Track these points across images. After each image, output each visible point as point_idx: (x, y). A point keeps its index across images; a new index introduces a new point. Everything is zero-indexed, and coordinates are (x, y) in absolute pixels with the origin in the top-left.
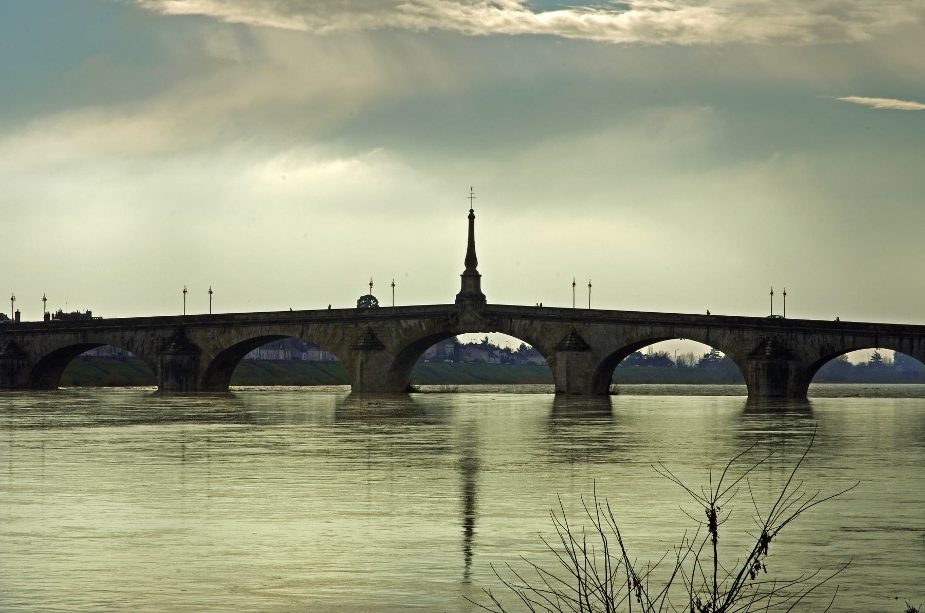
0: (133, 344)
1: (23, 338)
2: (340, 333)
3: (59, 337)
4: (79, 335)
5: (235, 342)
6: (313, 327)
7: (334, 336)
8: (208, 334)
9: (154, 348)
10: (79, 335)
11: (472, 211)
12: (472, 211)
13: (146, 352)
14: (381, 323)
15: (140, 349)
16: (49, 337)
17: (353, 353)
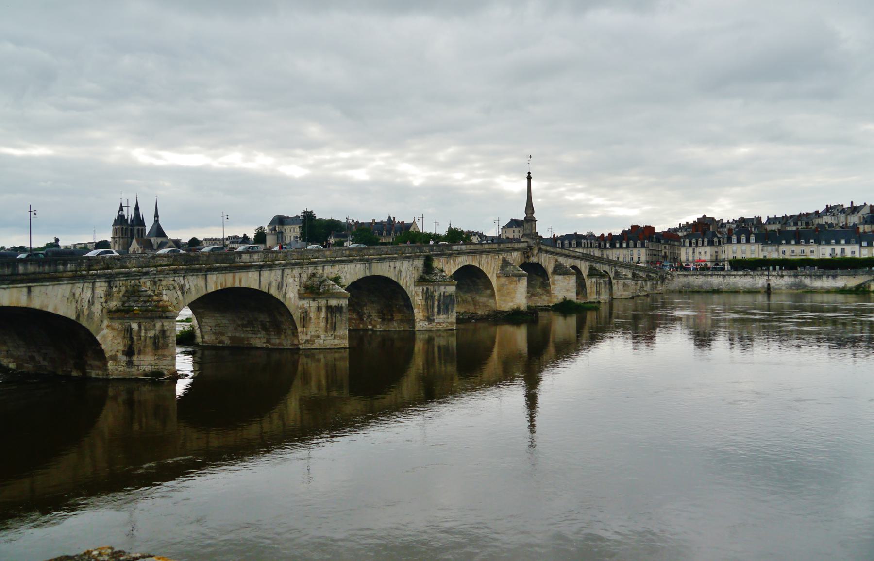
0: (401, 275)
1: (323, 270)
2: (493, 262)
3: (352, 266)
4: (366, 265)
5: (453, 271)
6: (484, 256)
7: (491, 266)
8: (441, 263)
9: (413, 279)
10: (366, 265)
11: (529, 173)
12: (529, 173)
13: (408, 285)
14: (506, 254)
15: (405, 281)
16: (344, 268)
17: (503, 280)
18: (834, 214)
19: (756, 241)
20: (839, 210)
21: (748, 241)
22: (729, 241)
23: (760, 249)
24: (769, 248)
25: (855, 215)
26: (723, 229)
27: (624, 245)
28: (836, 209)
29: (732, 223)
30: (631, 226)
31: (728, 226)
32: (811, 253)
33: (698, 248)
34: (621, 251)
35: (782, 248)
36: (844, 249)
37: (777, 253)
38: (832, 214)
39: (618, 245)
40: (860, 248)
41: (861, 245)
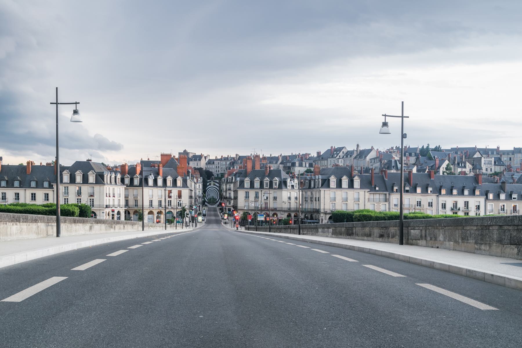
18: (340, 156)
19: (362, 187)
20: (345, 152)
21: (351, 185)
22: (326, 183)
23: (367, 197)
24: (377, 196)
25: (362, 159)
26: (211, 166)
27: (160, 182)
28: (342, 152)
29: (221, 160)
30: (162, 155)
31: (216, 162)
32: (429, 206)
33: (264, 191)
34: (155, 190)
35: (395, 198)
36: (468, 202)
37: (387, 204)
38: (338, 157)
39: (151, 182)
40: (485, 201)
41: (487, 198)
